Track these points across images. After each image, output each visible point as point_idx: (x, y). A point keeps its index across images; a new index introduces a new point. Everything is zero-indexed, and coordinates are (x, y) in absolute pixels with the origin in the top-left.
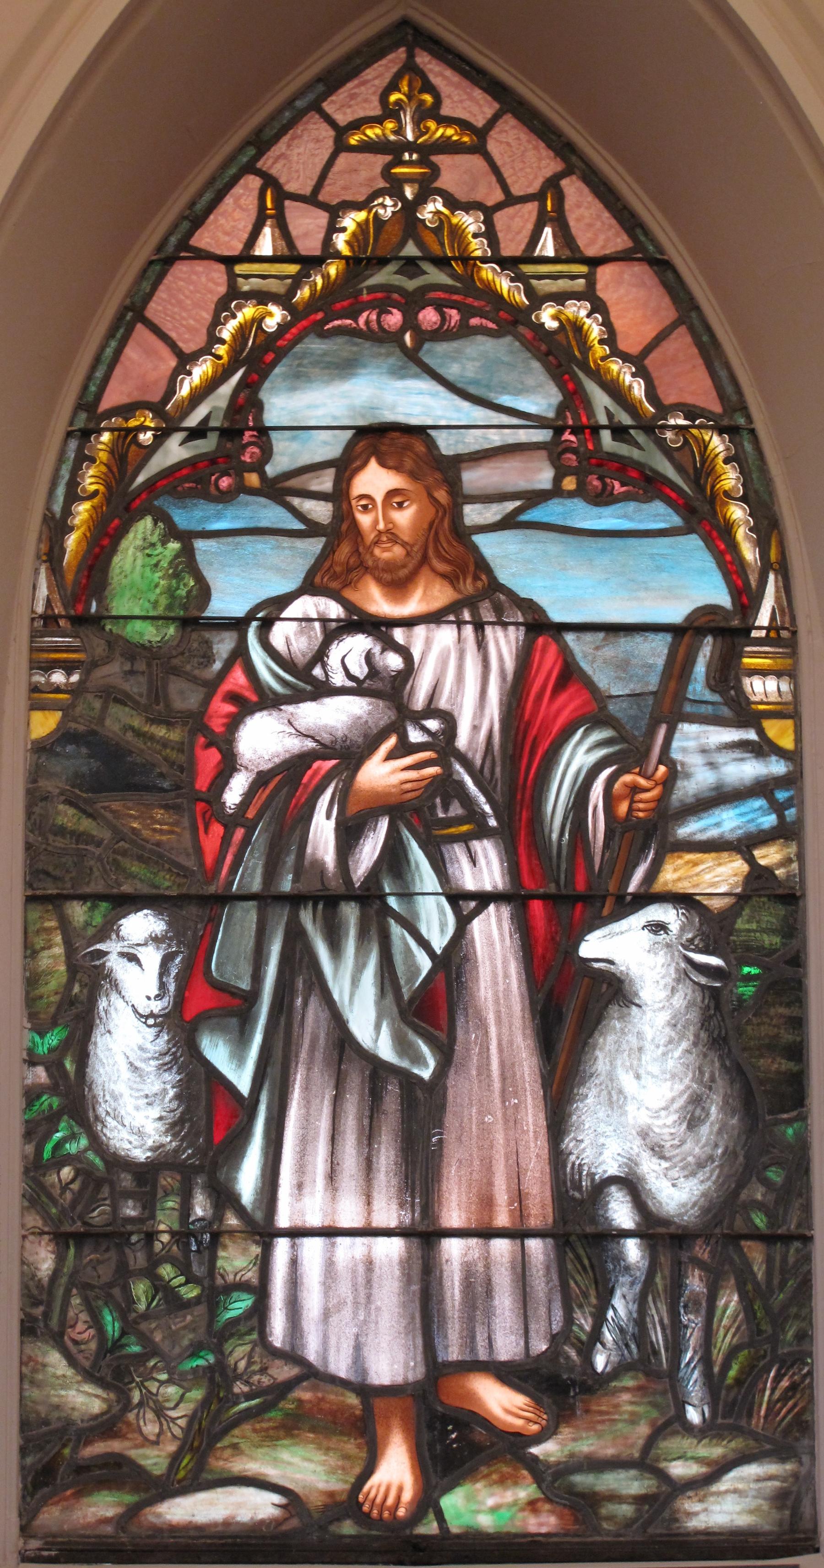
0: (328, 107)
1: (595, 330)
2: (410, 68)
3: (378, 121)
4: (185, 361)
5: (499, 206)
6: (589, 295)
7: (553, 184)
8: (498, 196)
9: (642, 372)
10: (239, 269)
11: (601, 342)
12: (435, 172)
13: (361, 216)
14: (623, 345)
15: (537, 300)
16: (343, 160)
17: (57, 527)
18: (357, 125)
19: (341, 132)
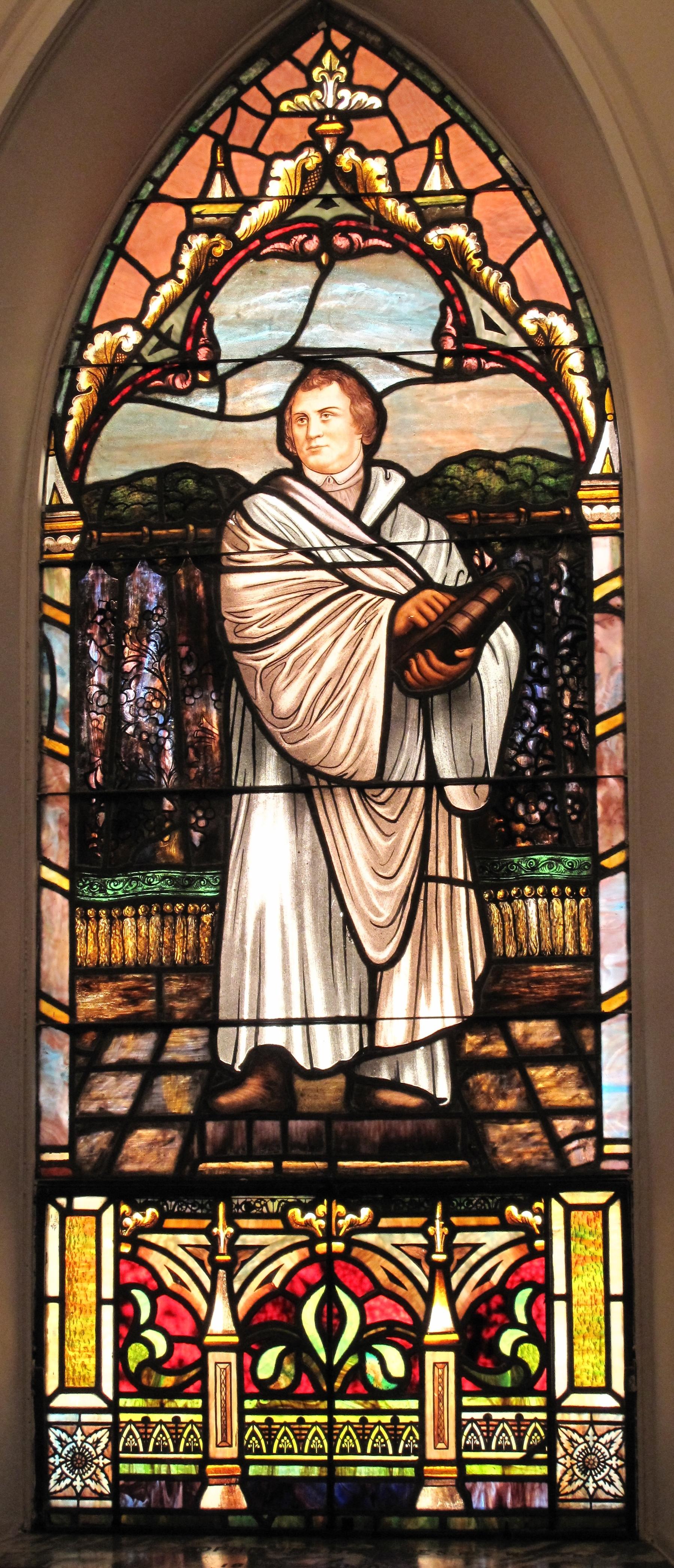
1: (471, 245)
5: (399, 152)
7: (440, 131)
9: (508, 277)
11: (476, 256)
13: (290, 165)
14: (492, 255)
15: (428, 225)
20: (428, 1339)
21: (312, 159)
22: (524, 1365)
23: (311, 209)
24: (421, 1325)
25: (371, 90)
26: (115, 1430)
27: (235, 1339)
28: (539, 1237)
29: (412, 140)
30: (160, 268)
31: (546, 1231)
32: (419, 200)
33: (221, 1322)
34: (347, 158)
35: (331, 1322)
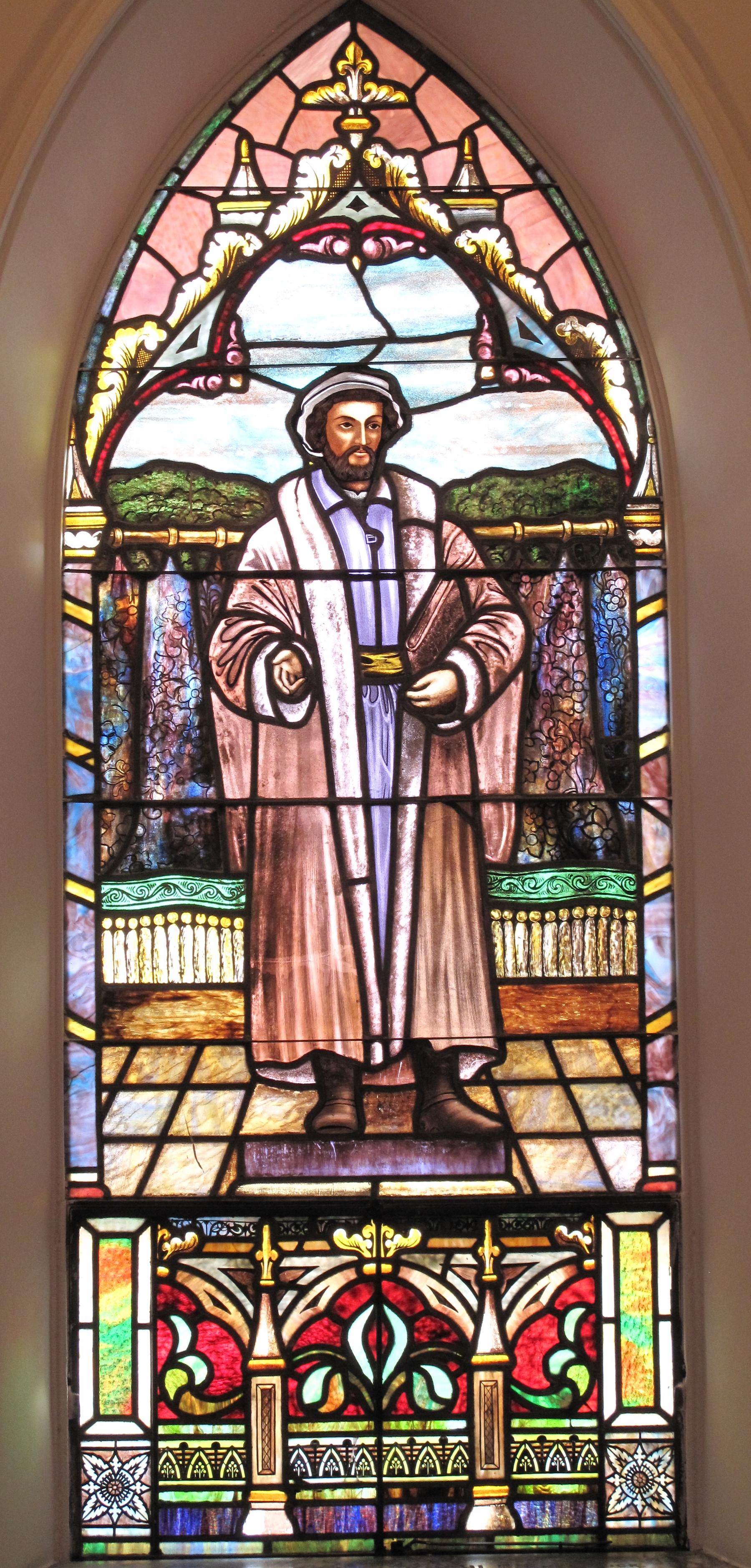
1: (504, 252)
2: (353, 37)
3: (330, 83)
4: (180, 281)
6: (498, 223)
7: (469, 132)
8: (426, 143)
9: (541, 284)
10: (221, 206)
15: (458, 227)
17: (82, 415)
18: (314, 86)
19: (299, 93)
20: (476, 1359)
21: (341, 157)
22: (573, 1385)
23: (341, 209)
24: (469, 1346)
25: (398, 86)
26: (154, 1454)
27: (281, 1362)
28: (589, 1257)
29: (441, 140)
30: (186, 267)
31: (596, 1251)
32: (448, 201)
33: (265, 1343)
34: (375, 155)
35: (378, 1342)
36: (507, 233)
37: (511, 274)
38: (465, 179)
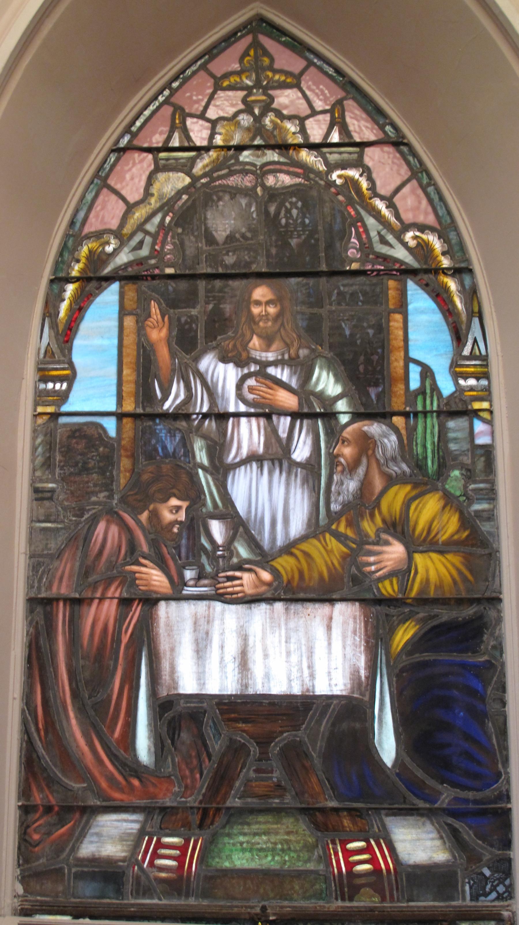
0: (210, 66)
1: (364, 184)
4: (130, 208)
9: (391, 205)
12: (272, 99)
15: (331, 167)
16: (220, 94)
18: (226, 76)
36: (367, 172)
37: (370, 198)
38: (335, 137)
